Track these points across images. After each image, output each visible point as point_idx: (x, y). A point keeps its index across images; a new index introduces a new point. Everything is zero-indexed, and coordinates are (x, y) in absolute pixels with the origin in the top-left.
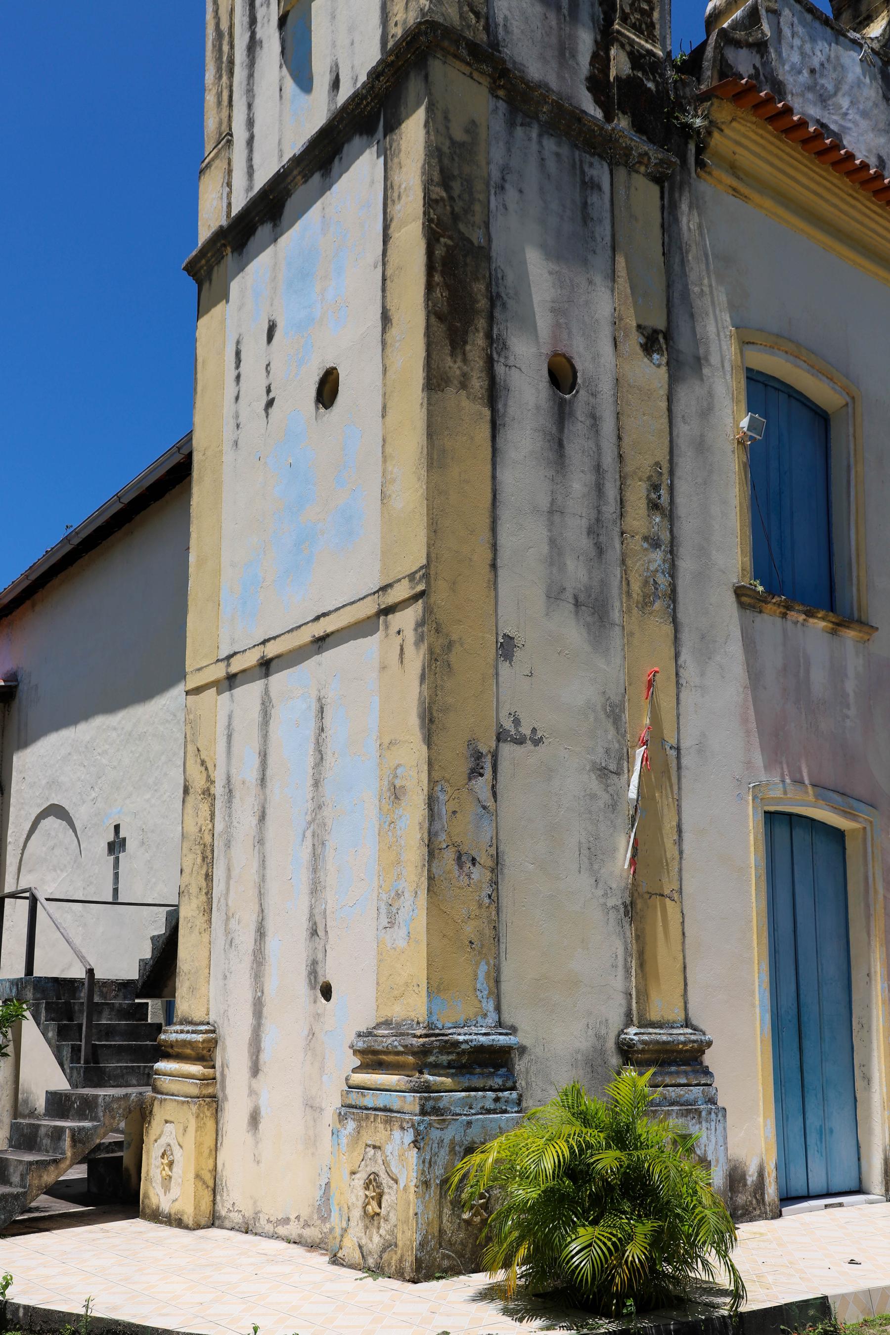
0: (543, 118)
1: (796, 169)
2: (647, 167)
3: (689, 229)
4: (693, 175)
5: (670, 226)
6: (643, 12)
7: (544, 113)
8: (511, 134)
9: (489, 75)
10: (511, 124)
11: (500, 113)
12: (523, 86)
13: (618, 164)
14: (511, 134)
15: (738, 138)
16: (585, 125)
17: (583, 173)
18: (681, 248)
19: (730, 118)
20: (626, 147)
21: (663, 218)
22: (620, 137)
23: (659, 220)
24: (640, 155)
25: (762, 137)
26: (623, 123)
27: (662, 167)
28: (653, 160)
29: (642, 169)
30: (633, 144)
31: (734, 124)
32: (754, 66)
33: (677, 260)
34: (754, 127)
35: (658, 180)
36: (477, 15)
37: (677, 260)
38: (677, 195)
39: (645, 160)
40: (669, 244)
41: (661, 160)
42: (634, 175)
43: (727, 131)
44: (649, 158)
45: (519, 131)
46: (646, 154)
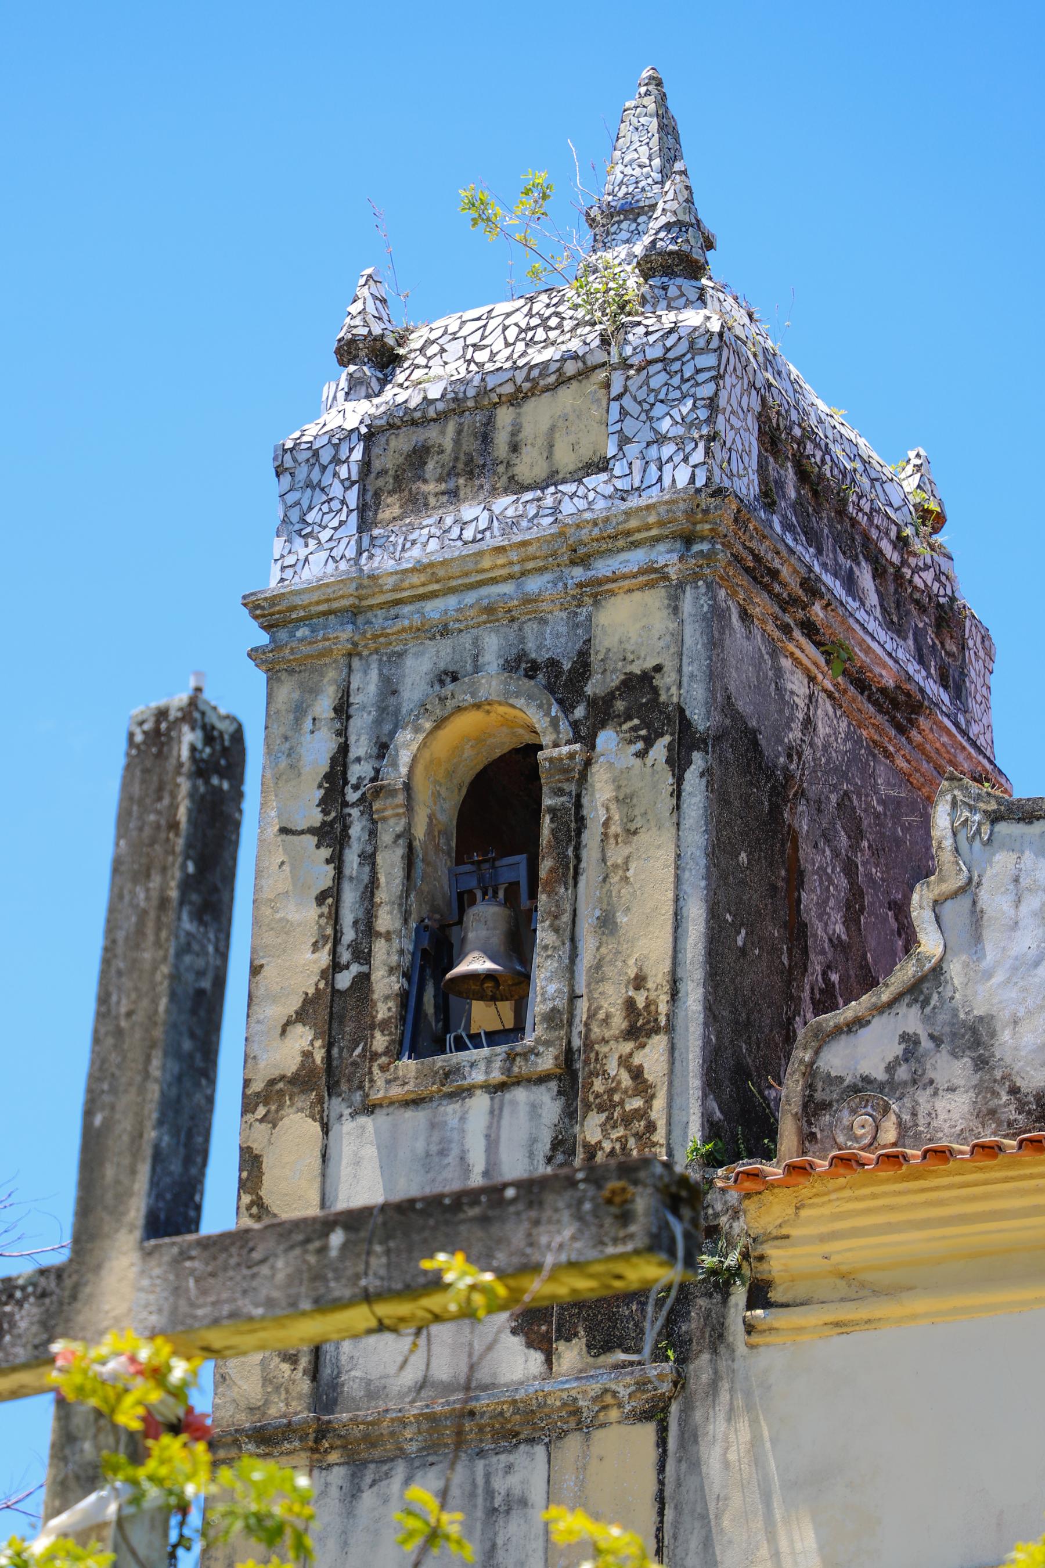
0: (412, 1448)
1: (986, 1197)
2: (620, 1406)
3: (726, 1465)
4: (741, 1349)
5: (679, 1484)
6: (628, 1120)
7: (411, 1440)
8: (350, 1513)
9: (302, 1449)
10: (353, 1493)
11: (334, 1491)
12: (361, 1427)
13: (563, 1434)
14: (350, 1513)
15: (824, 1229)
16: (483, 1414)
17: (490, 1493)
18: (704, 1517)
19: (791, 1211)
20: (564, 1404)
21: (661, 1483)
22: (545, 1396)
23: (652, 1487)
24: (595, 1399)
25: (874, 1196)
26: (571, 1355)
27: (648, 1391)
28: (623, 1393)
29: (614, 1414)
30: (573, 1393)
31: (804, 1213)
32: (905, 1037)
33: (694, 1543)
34: (847, 1193)
35: (655, 1413)
36: (292, 1359)
37: (694, 1543)
38: (698, 1415)
39: (609, 1399)
40: (676, 1524)
41: (637, 1383)
42: (598, 1435)
43: (794, 1232)
44: (615, 1394)
45: (368, 1498)
46: (606, 1391)
